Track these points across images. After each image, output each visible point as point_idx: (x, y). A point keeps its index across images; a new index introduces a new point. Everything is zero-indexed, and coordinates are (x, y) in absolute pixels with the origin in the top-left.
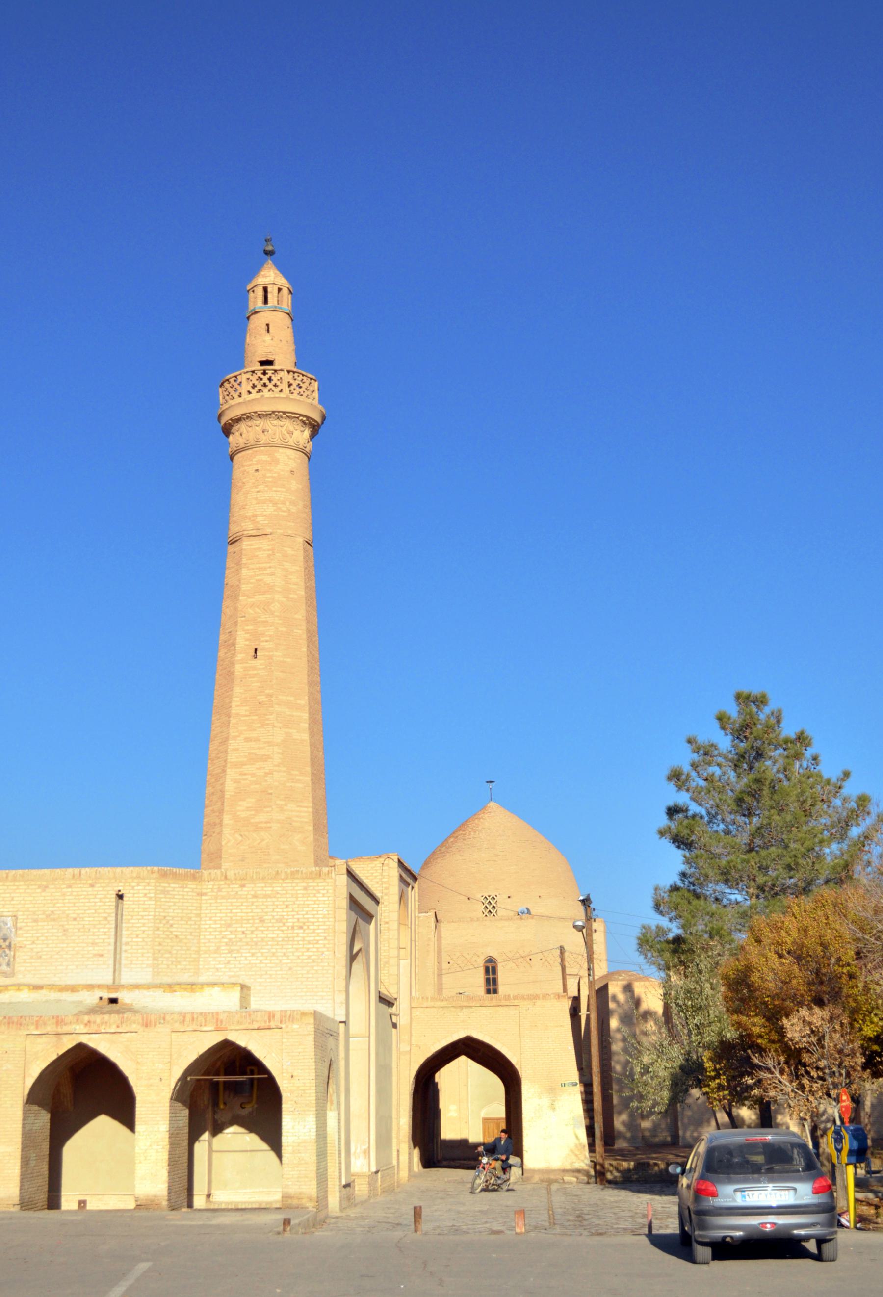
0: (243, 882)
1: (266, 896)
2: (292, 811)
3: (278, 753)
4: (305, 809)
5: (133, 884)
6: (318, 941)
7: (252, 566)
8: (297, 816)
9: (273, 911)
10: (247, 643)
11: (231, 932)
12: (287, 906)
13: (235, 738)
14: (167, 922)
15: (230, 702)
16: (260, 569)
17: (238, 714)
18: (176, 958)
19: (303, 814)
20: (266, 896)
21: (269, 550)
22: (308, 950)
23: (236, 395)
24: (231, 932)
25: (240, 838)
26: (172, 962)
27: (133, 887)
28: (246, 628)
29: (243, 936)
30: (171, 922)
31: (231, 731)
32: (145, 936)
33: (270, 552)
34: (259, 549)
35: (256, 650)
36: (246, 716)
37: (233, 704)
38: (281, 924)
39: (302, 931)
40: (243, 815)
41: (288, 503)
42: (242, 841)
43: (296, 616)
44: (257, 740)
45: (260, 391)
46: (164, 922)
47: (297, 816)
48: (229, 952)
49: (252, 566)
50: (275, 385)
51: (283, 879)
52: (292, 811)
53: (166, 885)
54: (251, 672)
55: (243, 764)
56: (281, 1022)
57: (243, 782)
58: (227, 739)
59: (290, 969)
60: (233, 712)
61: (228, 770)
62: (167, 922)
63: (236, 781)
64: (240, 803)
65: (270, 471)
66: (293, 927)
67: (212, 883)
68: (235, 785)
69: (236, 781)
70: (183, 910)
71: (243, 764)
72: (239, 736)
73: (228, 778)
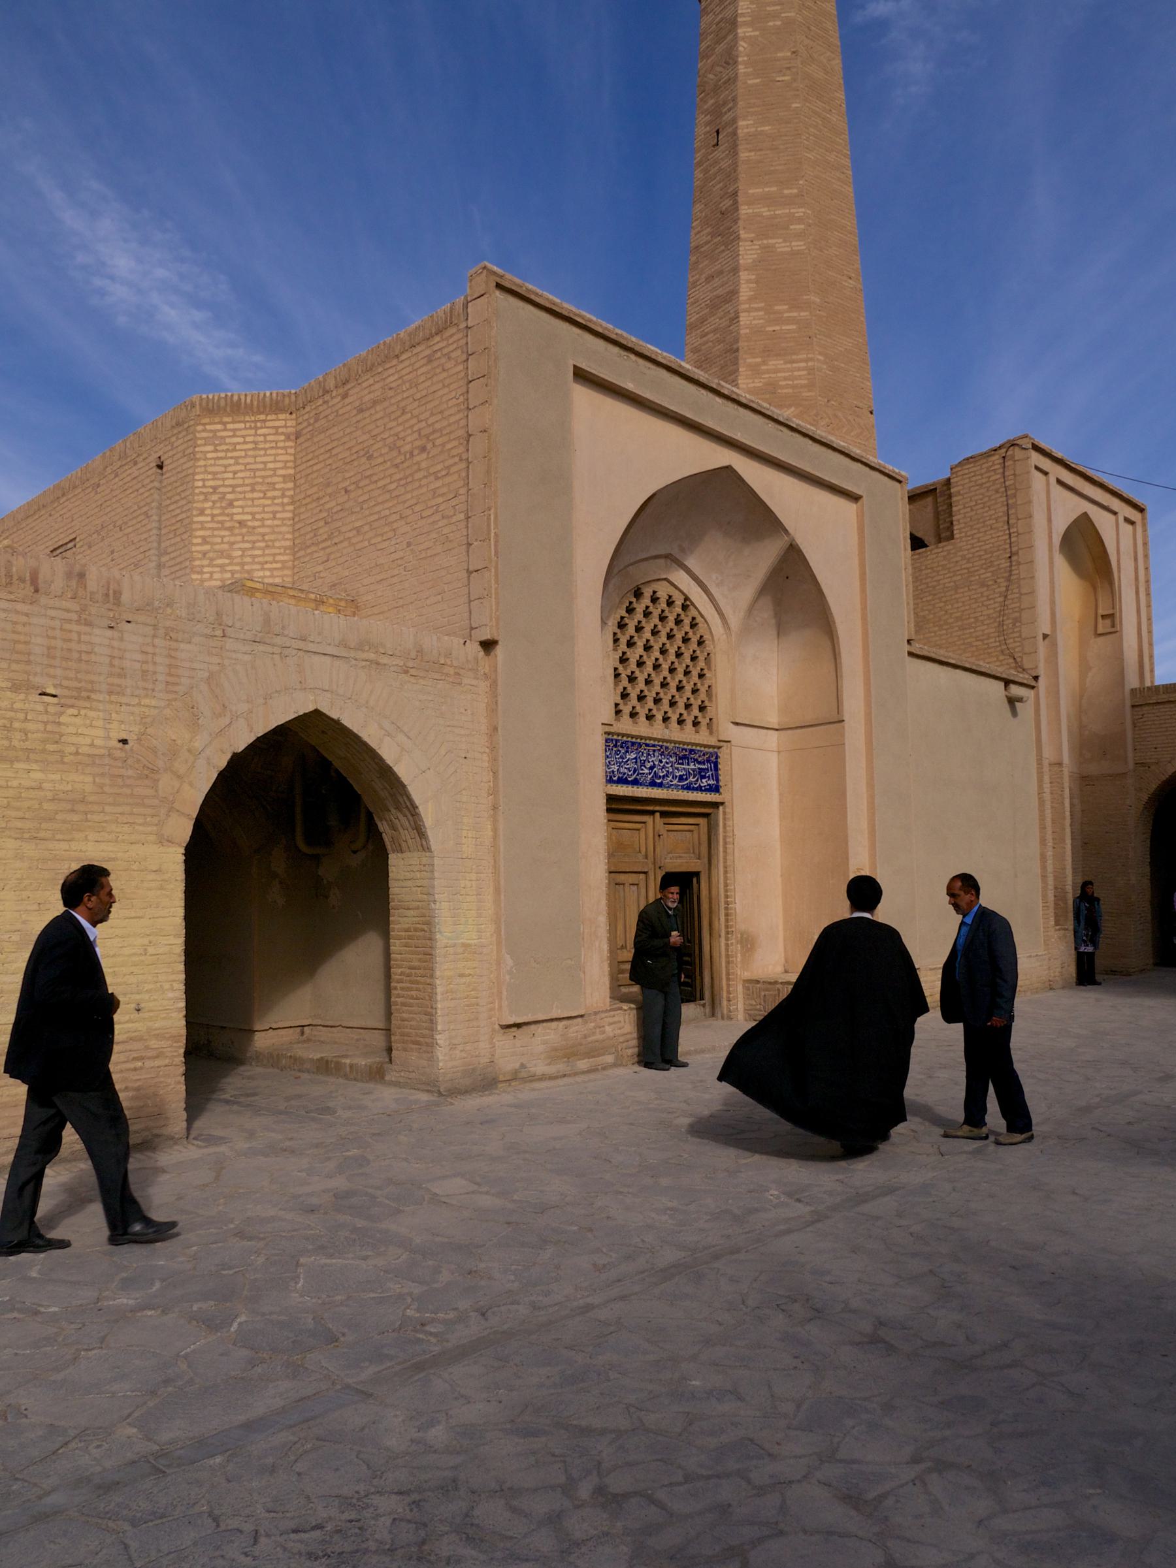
1: (375, 403)
2: (777, 371)
3: (749, 281)
4: (803, 365)
8: (785, 379)
14: (222, 499)
20: (375, 403)
30: (229, 496)
38: (395, 453)
39: (424, 456)
43: (780, 55)
44: (721, 272)
46: (215, 497)
47: (785, 379)
51: (397, 356)
52: (777, 371)
53: (219, 427)
55: (703, 320)
59: (409, 545)
62: (222, 499)
67: (308, 409)
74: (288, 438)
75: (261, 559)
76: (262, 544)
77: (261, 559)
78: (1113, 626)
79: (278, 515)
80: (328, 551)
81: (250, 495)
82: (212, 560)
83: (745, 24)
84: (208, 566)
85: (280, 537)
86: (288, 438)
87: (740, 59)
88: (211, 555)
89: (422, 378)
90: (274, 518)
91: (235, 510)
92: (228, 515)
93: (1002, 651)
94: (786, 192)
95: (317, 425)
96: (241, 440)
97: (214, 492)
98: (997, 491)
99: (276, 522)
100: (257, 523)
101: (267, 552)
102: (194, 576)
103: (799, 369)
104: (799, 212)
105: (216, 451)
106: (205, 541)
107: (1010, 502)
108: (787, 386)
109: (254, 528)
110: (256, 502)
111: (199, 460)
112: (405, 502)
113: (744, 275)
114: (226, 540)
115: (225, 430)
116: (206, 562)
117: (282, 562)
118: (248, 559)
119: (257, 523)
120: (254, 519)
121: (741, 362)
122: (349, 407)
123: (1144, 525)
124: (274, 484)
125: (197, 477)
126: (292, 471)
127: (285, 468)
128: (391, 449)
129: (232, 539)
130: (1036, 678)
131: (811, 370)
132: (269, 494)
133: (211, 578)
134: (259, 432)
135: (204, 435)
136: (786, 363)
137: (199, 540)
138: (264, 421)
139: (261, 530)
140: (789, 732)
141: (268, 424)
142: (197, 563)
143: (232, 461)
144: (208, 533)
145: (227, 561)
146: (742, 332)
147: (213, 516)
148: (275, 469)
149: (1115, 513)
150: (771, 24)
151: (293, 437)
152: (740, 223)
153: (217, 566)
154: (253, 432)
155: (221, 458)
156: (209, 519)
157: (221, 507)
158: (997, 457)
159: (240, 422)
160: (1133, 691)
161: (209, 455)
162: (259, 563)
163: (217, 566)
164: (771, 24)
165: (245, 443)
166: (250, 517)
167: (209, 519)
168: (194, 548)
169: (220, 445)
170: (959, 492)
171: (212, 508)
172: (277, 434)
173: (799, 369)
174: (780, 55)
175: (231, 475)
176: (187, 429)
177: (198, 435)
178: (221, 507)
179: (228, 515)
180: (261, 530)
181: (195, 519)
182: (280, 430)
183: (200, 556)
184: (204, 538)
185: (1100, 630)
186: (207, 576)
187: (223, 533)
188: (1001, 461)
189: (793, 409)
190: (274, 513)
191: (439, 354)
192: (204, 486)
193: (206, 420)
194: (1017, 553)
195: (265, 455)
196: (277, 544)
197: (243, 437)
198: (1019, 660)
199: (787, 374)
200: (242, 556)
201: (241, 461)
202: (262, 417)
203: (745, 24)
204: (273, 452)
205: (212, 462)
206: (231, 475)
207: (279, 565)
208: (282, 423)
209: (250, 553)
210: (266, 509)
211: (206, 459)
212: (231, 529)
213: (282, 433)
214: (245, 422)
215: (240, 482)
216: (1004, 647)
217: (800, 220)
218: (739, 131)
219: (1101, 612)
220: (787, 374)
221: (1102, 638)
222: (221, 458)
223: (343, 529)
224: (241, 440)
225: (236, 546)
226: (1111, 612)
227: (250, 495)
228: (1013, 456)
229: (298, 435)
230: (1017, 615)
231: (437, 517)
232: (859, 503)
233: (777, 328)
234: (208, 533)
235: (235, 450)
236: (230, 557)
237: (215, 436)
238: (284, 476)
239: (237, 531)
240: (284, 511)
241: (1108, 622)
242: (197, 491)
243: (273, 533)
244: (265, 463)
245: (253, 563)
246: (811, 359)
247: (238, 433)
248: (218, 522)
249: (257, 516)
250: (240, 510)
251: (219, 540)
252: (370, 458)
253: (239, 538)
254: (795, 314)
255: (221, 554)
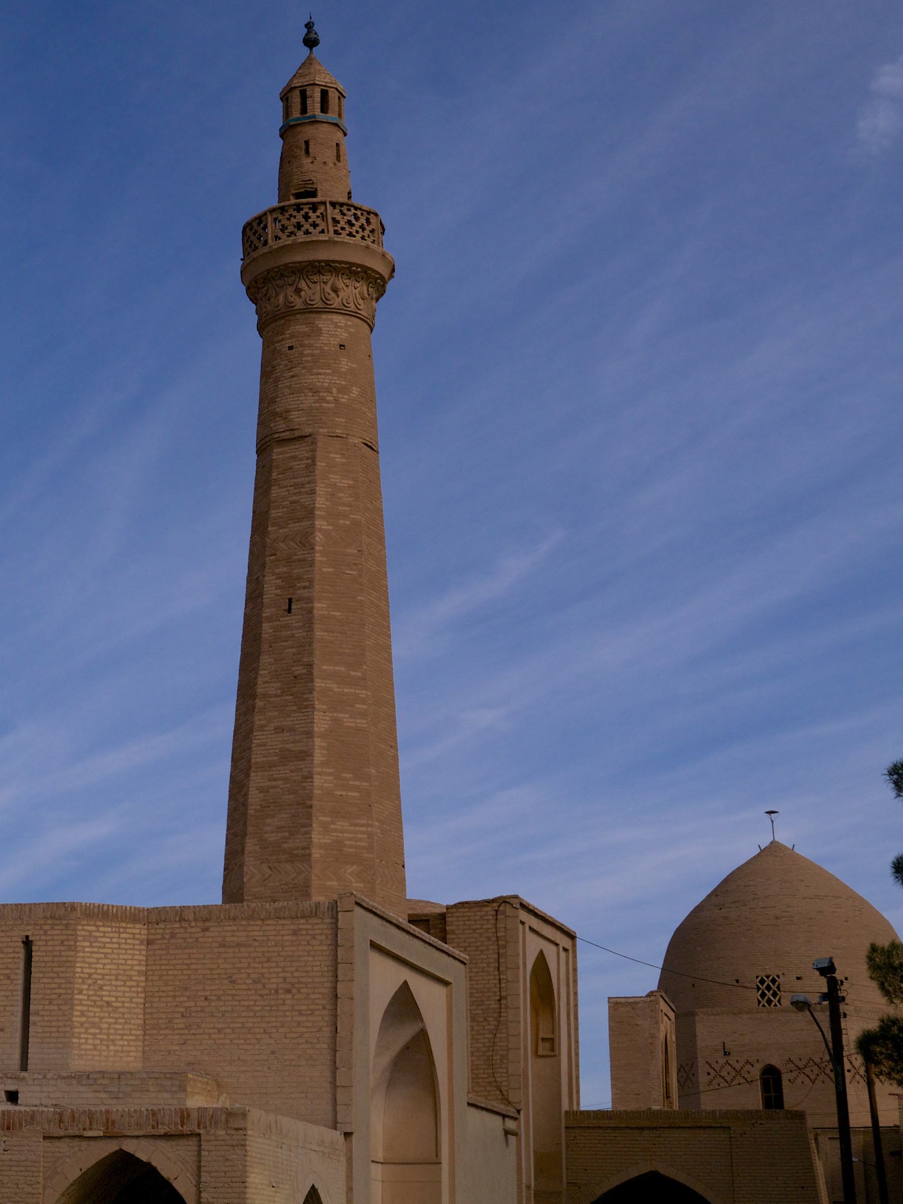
0: (207, 924)
1: (239, 945)
2: (343, 832)
3: (321, 747)
5: (46, 927)
6: (313, 1010)
7: (284, 483)
8: (350, 839)
9: (249, 967)
10: (279, 592)
11: (188, 997)
12: (268, 960)
13: (262, 728)
15: (256, 678)
16: (296, 485)
17: (265, 696)
18: (108, 1034)
19: (359, 836)
21: (307, 458)
22: (299, 1024)
23: (259, 245)
24: (188, 997)
25: (269, 871)
26: (102, 1040)
27: (46, 931)
28: (277, 571)
29: (206, 1003)
30: (99, 982)
31: (256, 718)
32: (61, 1002)
33: (309, 461)
34: (294, 458)
35: (290, 600)
36: (276, 696)
37: (260, 680)
38: (259, 986)
39: (289, 996)
40: (272, 837)
41: (334, 391)
42: (270, 876)
44: (291, 730)
45: (292, 233)
46: (90, 981)
47: (350, 839)
48: (186, 1028)
49: (284, 483)
50: (315, 225)
51: (262, 920)
52: (343, 832)
53: (93, 928)
54: (284, 633)
55: (271, 765)
56: (199, 1126)
57: (271, 791)
58: (251, 731)
59: (273, 1053)
60: (259, 690)
61: (252, 774)
62: (95, 983)
63: (261, 790)
64: (268, 821)
65: (310, 346)
66: (277, 991)
67: (162, 925)
68: (261, 795)
69: (261, 790)
70: (118, 964)
71: (271, 765)
72: (266, 726)
73: (252, 784)
74: (142, 943)
75: (121, 1032)
76: (123, 1021)
77: (121, 1032)
78: (553, 1050)
79: (134, 1000)
80: (185, 1037)
81: (114, 983)
82: (87, 1029)
83: (321, 517)
84: (85, 1033)
85: (135, 1016)
86: (142, 943)
87: (317, 548)
88: (87, 1025)
89: (287, 943)
90: (131, 1002)
91: (104, 993)
92: (99, 996)
93: (490, 1083)
94: (352, 673)
95: (172, 941)
96: (109, 940)
97: (89, 977)
98: (489, 939)
99: (133, 1005)
100: (119, 1005)
101: (126, 1027)
102: (75, 1040)
103: (361, 833)
104: (363, 693)
105: (91, 946)
106: (82, 1014)
107: (501, 951)
108: (351, 846)
109: (117, 1008)
110: (119, 989)
111: (79, 952)
112: (269, 1023)
113: (318, 742)
114: (97, 1014)
115: (98, 931)
116: (83, 1030)
117: (136, 1035)
118: (112, 1031)
119: (119, 1005)
120: (117, 1001)
121: (314, 818)
122: (210, 940)
123: (574, 952)
124: (131, 976)
125: (77, 965)
126: (144, 968)
127: (139, 965)
128: (254, 982)
129: (102, 1015)
130: (519, 1111)
131: (370, 835)
132: (128, 983)
133: (86, 1043)
134: (122, 936)
135: (83, 933)
136: (351, 825)
137: (78, 1013)
138: (125, 928)
139: (122, 1010)
140: (401, 1166)
141: (128, 930)
142: (77, 1030)
143: (102, 956)
144: (85, 1008)
145: (98, 1031)
146: (315, 792)
147: (89, 996)
148: (132, 965)
149: (557, 945)
150: (342, 522)
151: (145, 943)
152: (315, 694)
153: (91, 1034)
154: (117, 935)
155: (96, 953)
156: (85, 997)
157: (94, 990)
158: (490, 909)
159: (108, 927)
160: (566, 1112)
161: (87, 949)
162: (120, 1035)
163: (91, 1034)
164: (342, 522)
165: (112, 943)
166: (114, 999)
167: (85, 997)
168: (74, 1019)
169: (95, 942)
170: (453, 931)
171: (88, 990)
172: (134, 938)
173: (361, 833)
174: (349, 551)
175: (101, 966)
176: (67, 925)
177: (78, 933)
178: (94, 990)
179: (99, 996)
180: (122, 1010)
181: (76, 997)
182: (137, 936)
183: (79, 1025)
184: (82, 1012)
185: (540, 1052)
186: (83, 1041)
187: (95, 1009)
188: (494, 913)
189: (355, 867)
190: (131, 998)
191: (304, 932)
192: (82, 972)
193: (85, 922)
194: (506, 998)
195: (126, 954)
196: (133, 1022)
197: (111, 938)
198: (505, 1093)
199: (351, 835)
200: (108, 1028)
201: (109, 956)
202: (124, 925)
203: (321, 517)
204: (131, 952)
205: (89, 955)
206: (101, 966)
207: (134, 1038)
208: (137, 931)
209: (114, 1026)
210: (126, 994)
211: (84, 952)
212: (101, 1007)
213: (138, 939)
214: (112, 927)
215: (107, 972)
216: (492, 1079)
217: (363, 701)
218: (315, 611)
219: (542, 1035)
220: (351, 835)
221: (541, 1061)
222: (96, 953)
223: (203, 1025)
224: (109, 940)
225: (104, 1020)
226: (549, 1036)
227: (114, 983)
228: (504, 913)
229: (149, 942)
230: (505, 1053)
231: (302, 1040)
232: (449, 987)
233: (344, 793)
234: (85, 1008)
235: (104, 947)
236: (100, 1029)
237: (90, 935)
238: (139, 971)
239: (105, 1009)
240: (138, 997)
241: (547, 1045)
242: (77, 975)
243: (130, 1013)
244: (126, 960)
245: (116, 1034)
246: (371, 826)
247: (107, 935)
248: (92, 1001)
249: (120, 999)
250: (107, 993)
251: (92, 1014)
252: (233, 982)
253: (106, 1015)
254: (358, 783)
255: (94, 1025)
